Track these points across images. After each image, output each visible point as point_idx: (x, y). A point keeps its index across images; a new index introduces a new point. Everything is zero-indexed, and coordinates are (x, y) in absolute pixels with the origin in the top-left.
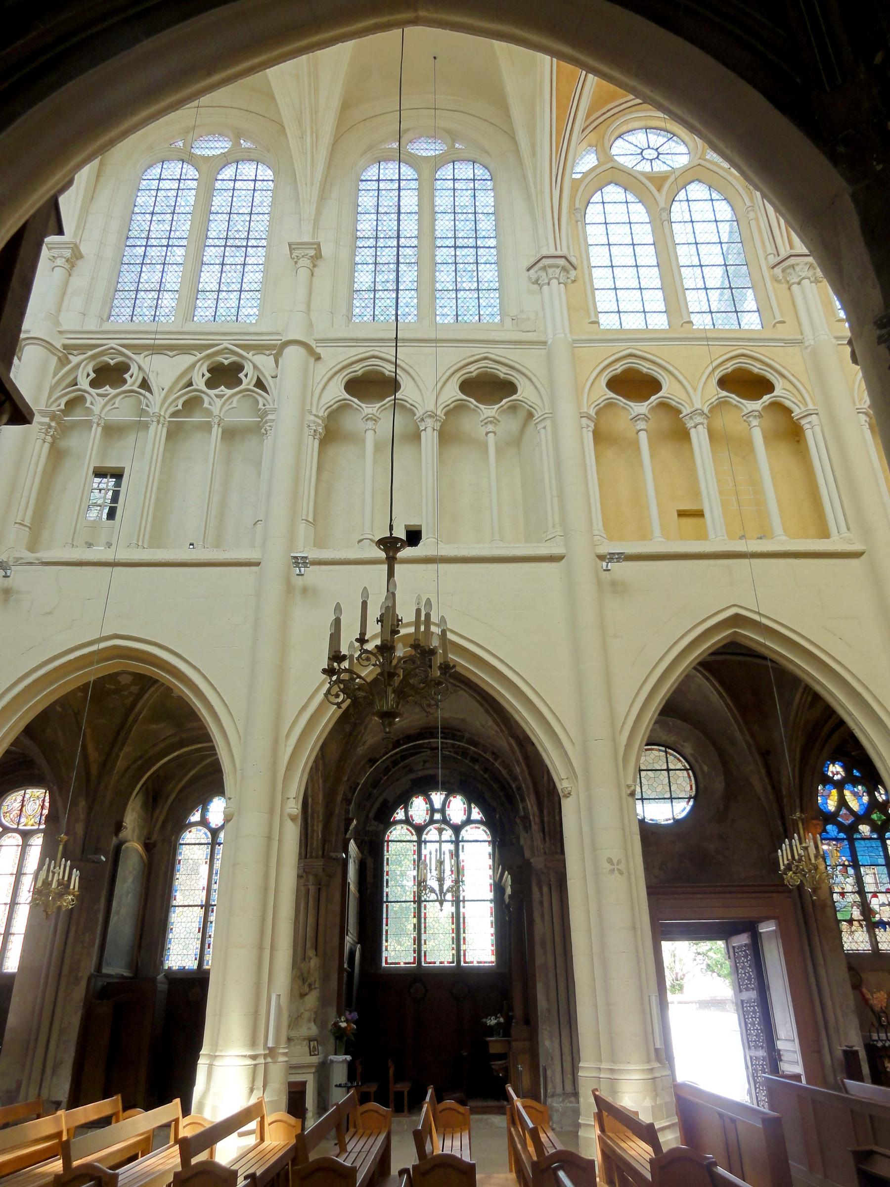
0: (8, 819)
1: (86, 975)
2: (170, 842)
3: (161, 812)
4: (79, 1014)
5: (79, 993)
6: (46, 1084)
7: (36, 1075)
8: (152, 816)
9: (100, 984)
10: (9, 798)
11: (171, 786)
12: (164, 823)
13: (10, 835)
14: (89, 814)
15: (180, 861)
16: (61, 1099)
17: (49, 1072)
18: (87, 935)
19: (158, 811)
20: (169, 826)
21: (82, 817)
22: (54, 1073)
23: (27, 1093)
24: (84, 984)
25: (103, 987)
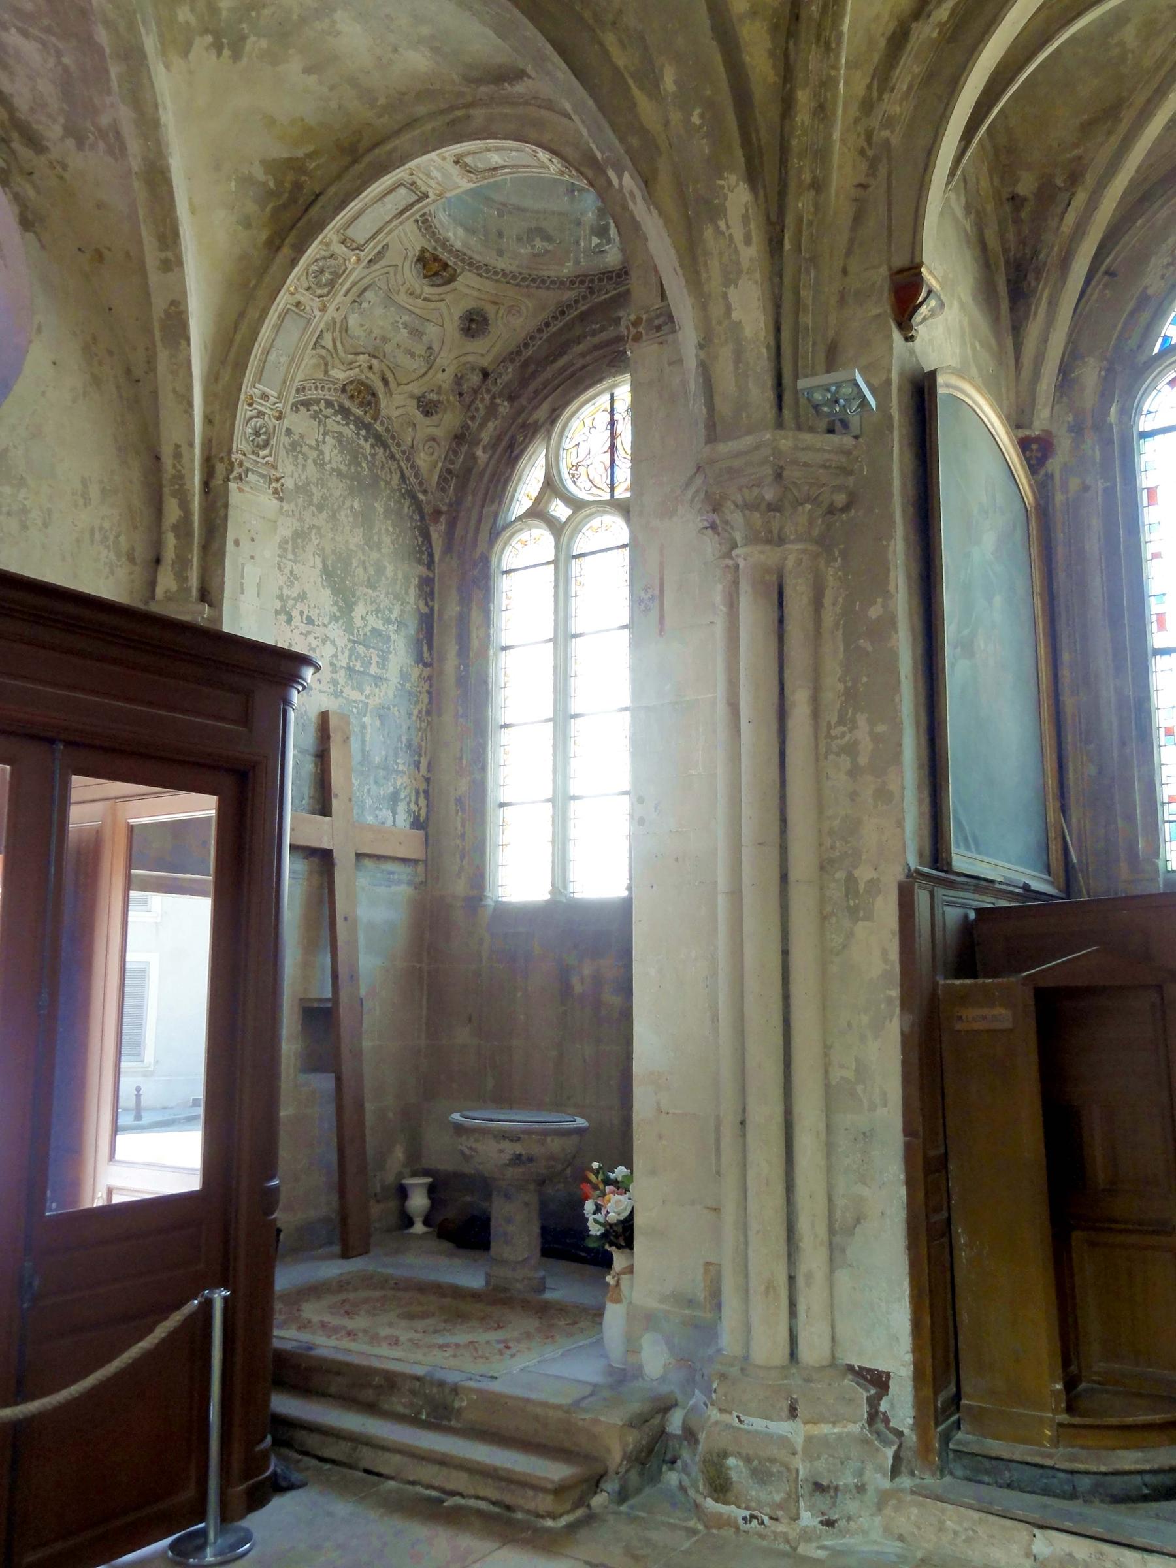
0: (583, 482)
1: (892, 876)
2: (1101, 425)
3: (1050, 323)
4: (894, 1028)
5: (875, 947)
6: (811, 1299)
7: (766, 1261)
8: (1018, 347)
9: (953, 915)
10: (575, 424)
11: (1070, 218)
12: (1065, 371)
13: (595, 522)
14: (775, 245)
15: (1152, 492)
16: (881, 1365)
17: (813, 1259)
18: (862, 719)
19: (1033, 330)
20: (1090, 374)
21: (751, 253)
22: (835, 1254)
23: (748, 1328)
24: (887, 910)
25: (967, 930)
